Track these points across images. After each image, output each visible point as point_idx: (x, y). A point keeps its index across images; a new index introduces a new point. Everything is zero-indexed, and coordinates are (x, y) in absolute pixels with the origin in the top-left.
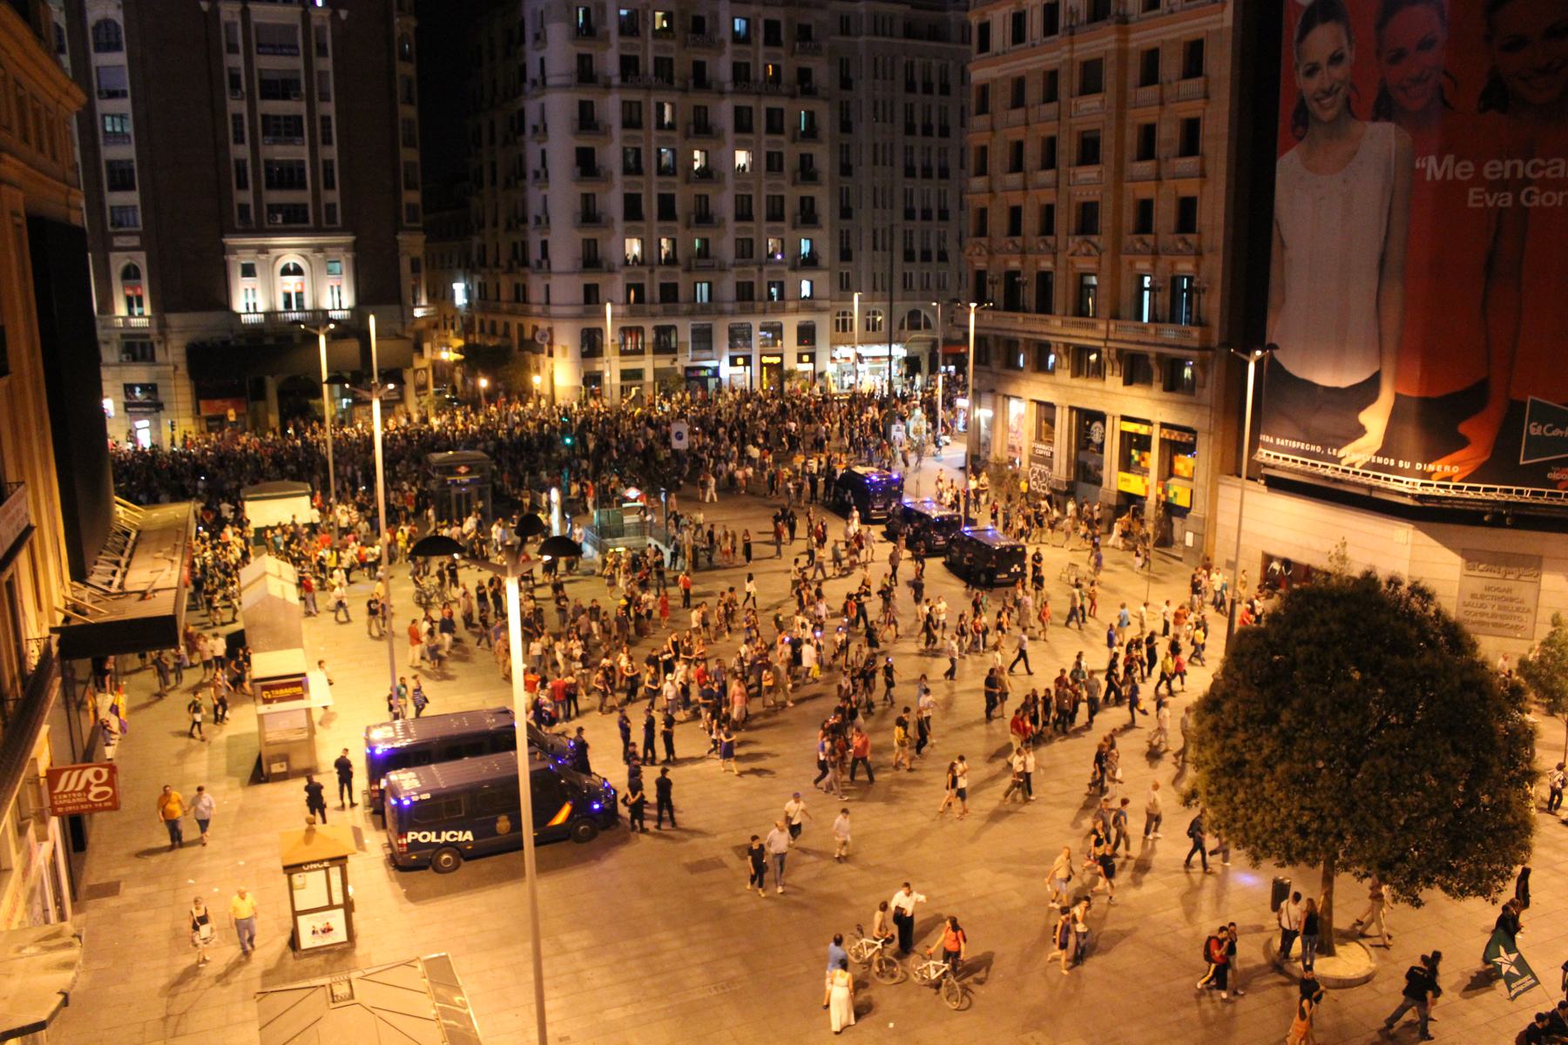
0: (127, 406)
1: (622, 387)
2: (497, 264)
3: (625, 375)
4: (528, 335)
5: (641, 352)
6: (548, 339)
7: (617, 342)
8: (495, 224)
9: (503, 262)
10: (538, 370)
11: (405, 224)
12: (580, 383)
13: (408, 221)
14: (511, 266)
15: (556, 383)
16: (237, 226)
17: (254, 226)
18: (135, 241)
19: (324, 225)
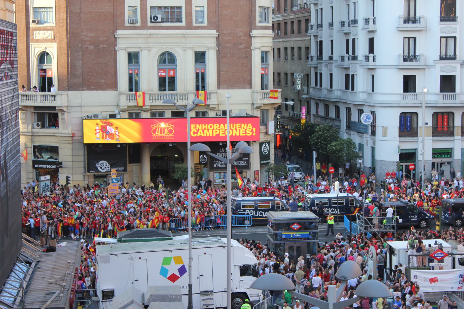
0: (34, 162)
1: (433, 164)
2: (331, 58)
3: (436, 153)
4: (354, 118)
5: (452, 134)
6: (371, 120)
7: (430, 124)
8: (331, 25)
9: (336, 57)
10: (361, 146)
11: (258, 24)
12: (397, 159)
13: (261, 22)
14: (343, 59)
15: (378, 157)
16: (127, 24)
17: (139, 24)
18: (49, 34)
19: (194, 24)
